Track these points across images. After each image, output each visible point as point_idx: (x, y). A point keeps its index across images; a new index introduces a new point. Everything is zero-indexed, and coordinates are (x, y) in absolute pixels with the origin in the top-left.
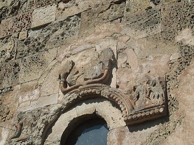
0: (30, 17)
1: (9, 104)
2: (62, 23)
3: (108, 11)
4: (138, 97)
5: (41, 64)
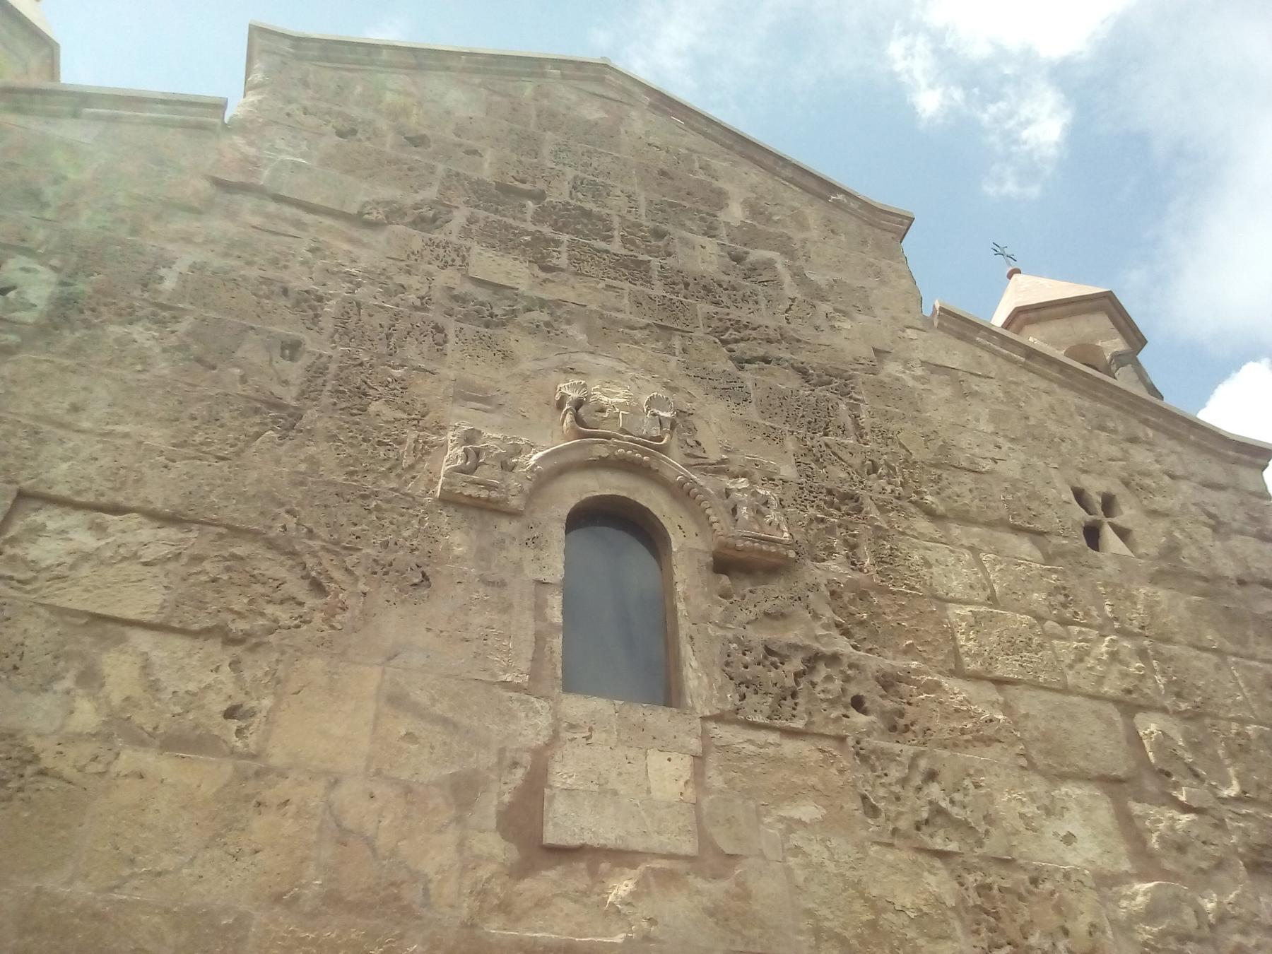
1: (425, 396)
2: (543, 304)
3: (642, 331)
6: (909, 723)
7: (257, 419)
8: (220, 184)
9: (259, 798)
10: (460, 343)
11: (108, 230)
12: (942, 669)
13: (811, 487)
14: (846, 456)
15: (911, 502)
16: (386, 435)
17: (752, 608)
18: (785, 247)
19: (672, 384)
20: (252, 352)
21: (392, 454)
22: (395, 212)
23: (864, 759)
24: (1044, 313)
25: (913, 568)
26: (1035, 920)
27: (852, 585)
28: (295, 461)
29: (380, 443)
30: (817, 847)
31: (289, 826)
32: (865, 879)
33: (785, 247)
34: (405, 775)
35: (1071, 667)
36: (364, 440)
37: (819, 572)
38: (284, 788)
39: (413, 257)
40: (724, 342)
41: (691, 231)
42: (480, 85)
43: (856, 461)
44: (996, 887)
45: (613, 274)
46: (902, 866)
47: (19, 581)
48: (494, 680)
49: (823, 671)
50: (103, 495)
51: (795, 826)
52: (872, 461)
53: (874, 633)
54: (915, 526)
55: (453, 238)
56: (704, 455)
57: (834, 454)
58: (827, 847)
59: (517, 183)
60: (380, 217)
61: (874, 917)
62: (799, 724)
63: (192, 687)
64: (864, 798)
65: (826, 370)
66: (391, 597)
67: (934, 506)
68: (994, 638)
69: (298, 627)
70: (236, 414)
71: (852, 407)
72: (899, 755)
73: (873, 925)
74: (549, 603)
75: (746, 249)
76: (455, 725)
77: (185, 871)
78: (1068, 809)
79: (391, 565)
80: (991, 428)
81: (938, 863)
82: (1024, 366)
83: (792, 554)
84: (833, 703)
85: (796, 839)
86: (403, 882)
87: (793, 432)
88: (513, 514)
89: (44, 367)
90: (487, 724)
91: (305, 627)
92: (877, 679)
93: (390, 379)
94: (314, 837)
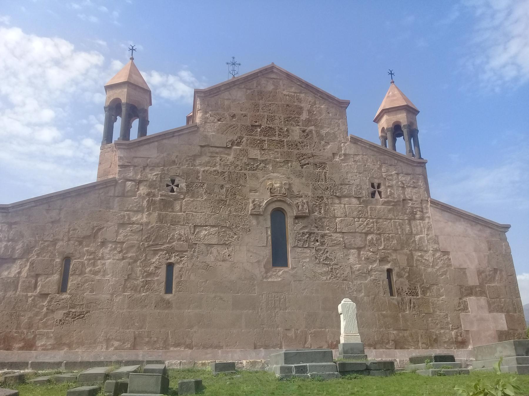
24: (390, 110)
29: (240, 205)
43: (324, 188)
49: (312, 235)
56: (294, 194)
62: (307, 246)
68: (344, 224)
73: (314, 275)
81: (326, 265)
82: (369, 148)
84: (313, 241)
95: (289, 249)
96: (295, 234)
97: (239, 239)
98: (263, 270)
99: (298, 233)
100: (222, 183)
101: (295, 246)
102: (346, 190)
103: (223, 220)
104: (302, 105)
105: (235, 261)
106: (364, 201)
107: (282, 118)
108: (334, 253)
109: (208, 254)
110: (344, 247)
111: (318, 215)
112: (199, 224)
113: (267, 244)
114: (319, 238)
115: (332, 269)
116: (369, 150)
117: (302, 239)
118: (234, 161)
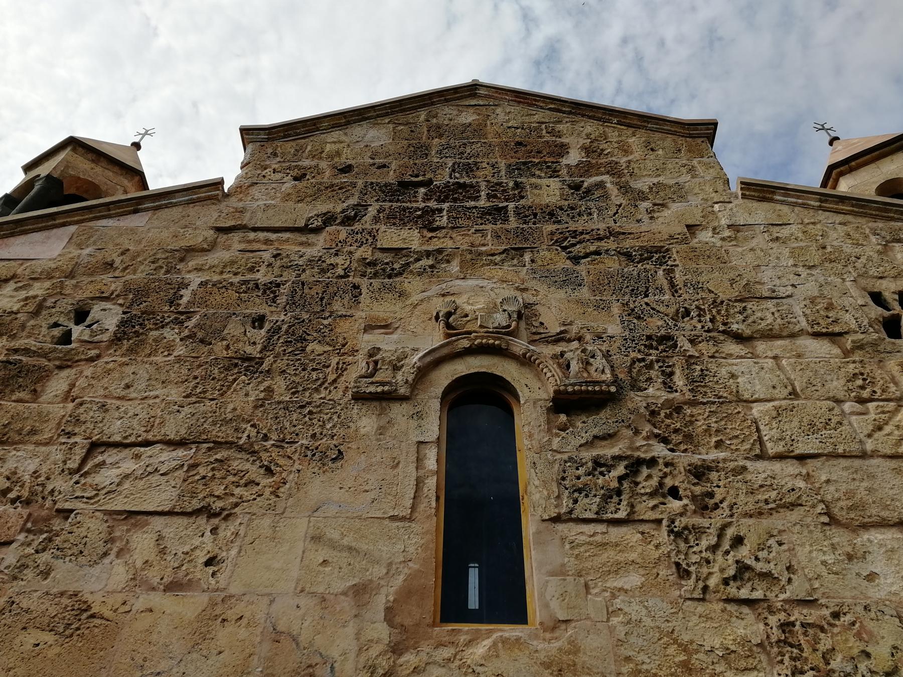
0: (376, 234)
2: (428, 254)
4: (568, 366)
5: (398, 295)
6: (718, 501)
7: (236, 371)
8: (219, 230)
9: (223, 616)
10: (370, 293)
11: (153, 275)
12: (748, 455)
13: (634, 337)
14: (662, 309)
15: (719, 332)
16: (318, 363)
17: (584, 435)
18: (614, 170)
19: (522, 287)
20: (234, 329)
21: (321, 375)
22: (328, 219)
23: (678, 535)
24: (853, 163)
25: (720, 382)
26: (837, 648)
27: (668, 403)
28: (257, 392)
29: (314, 370)
30: (637, 608)
31: (243, 633)
32: (677, 629)
33: (614, 170)
34: (321, 589)
35: (869, 436)
36: (304, 370)
37: (640, 399)
38: (240, 608)
39: (339, 244)
40: (564, 248)
41: (539, 177)
42: (389, 123)
43: (671, 310)
44: (798, 623)
45: (480, 221)
46: (713, 615)
47: (87, 498)
48: (386, 516)
49: (645, 472)
50: (140, 436)
51: (618, 594)
52: (685, 308)
53: (689, 438)
54: (722, 350)
55: (368, 226)
57: (653, 309)
58: (644, 606)
59: (412, 179)
60: (319, 224)
61: (686, 658)
62: (622, 514)
63: (187, 548)
64: (678, 565)
65: (647, 250)
66: (316, 470)
67: (740, 331)
68: (795, 423)
69: (255, 499)
70: (222, 370)
71: (669, 272)
72: (708, 528)
74: (427, 455)
75: (581, 179)
76: (358, 552)
77: (175, 670)
78: (870, 553)
79: (317, 448)
80: (791, 262)
81: (746, 610)
82: (820, 208)
83: (613, 389)
84: (652, 495)
85: (618, 603)
86: (317, 664)
87: (618, 300)
88: (404, 399)
89: (111, 365)
90: (380, 547)
91: (258, 499)
92: (689, 471)
93: (322, 327)
94: (258, 639)
95: (530, 526)
96: (557, 466)
97: (282, 490)
98: (381, 631)
99: (571, 459)
100: (262, 311)
101: (559, 514)
102: (769, 316)
103: (226, 422)
104: (564, 140)
105: (233, 590)
106: (859, 346)
107: (502, 165)
108: (780, 544)
109: (105, 554)
110: (825, 519)
111: (658, 393)
112: (117, 438)
113: (413, 508)
114: (681, 478)
115: (786, 626)
116: (820, 212)
117: (596, 484)
118: (321, 257)
